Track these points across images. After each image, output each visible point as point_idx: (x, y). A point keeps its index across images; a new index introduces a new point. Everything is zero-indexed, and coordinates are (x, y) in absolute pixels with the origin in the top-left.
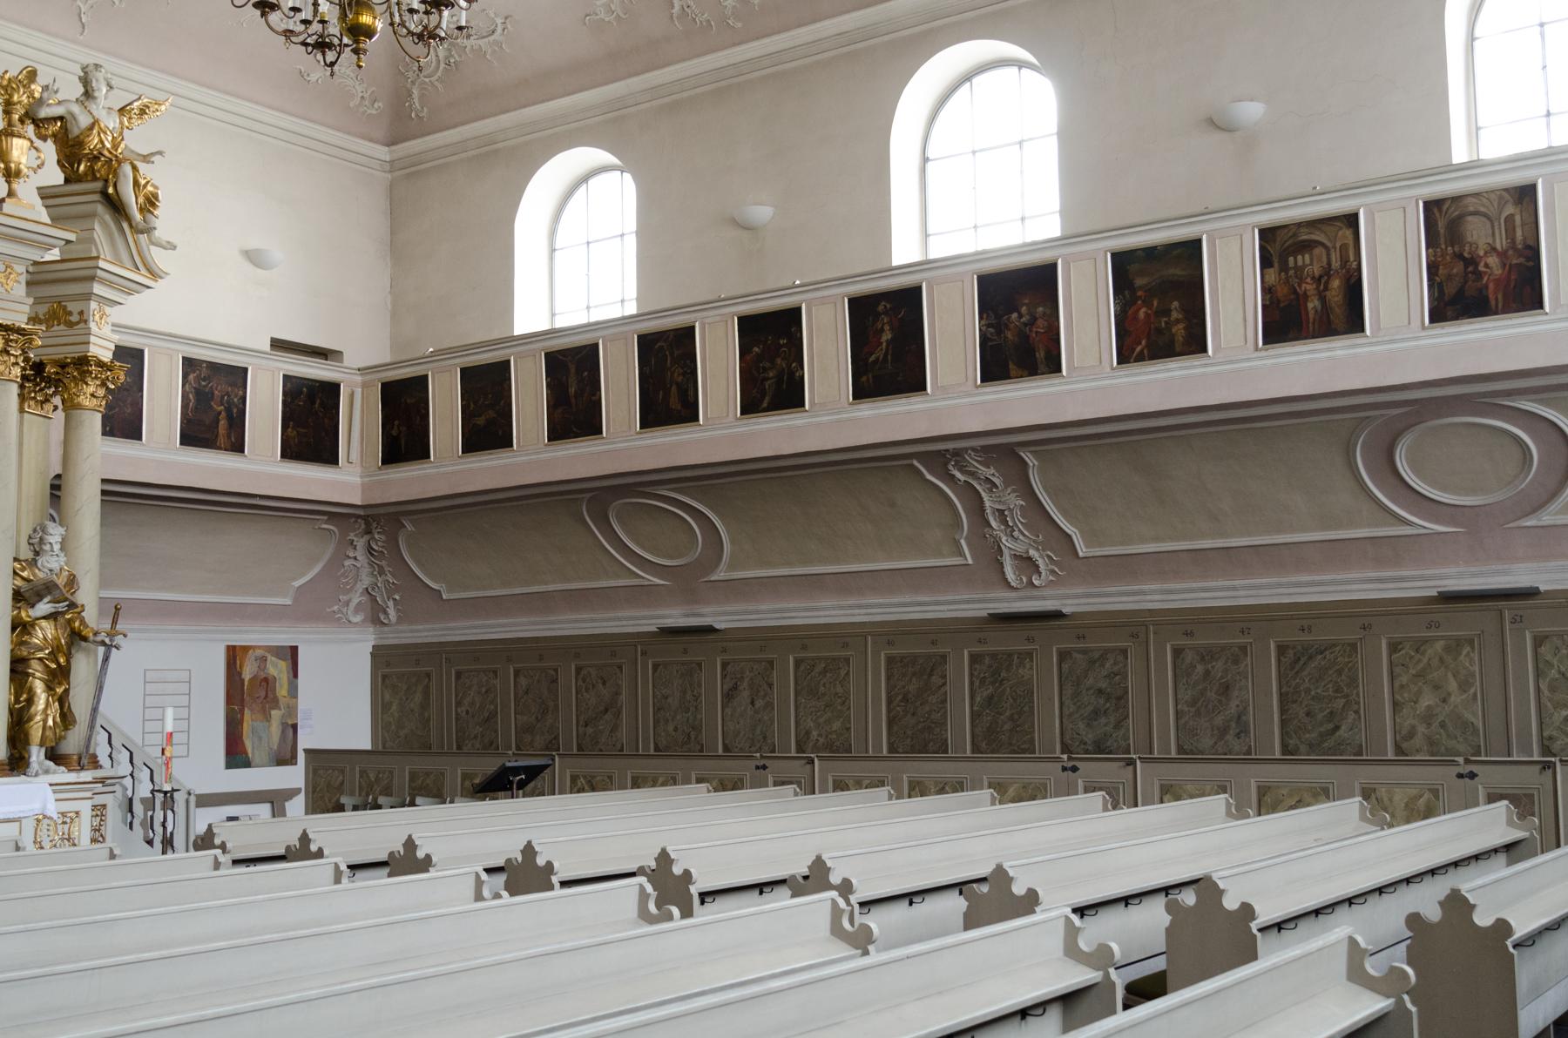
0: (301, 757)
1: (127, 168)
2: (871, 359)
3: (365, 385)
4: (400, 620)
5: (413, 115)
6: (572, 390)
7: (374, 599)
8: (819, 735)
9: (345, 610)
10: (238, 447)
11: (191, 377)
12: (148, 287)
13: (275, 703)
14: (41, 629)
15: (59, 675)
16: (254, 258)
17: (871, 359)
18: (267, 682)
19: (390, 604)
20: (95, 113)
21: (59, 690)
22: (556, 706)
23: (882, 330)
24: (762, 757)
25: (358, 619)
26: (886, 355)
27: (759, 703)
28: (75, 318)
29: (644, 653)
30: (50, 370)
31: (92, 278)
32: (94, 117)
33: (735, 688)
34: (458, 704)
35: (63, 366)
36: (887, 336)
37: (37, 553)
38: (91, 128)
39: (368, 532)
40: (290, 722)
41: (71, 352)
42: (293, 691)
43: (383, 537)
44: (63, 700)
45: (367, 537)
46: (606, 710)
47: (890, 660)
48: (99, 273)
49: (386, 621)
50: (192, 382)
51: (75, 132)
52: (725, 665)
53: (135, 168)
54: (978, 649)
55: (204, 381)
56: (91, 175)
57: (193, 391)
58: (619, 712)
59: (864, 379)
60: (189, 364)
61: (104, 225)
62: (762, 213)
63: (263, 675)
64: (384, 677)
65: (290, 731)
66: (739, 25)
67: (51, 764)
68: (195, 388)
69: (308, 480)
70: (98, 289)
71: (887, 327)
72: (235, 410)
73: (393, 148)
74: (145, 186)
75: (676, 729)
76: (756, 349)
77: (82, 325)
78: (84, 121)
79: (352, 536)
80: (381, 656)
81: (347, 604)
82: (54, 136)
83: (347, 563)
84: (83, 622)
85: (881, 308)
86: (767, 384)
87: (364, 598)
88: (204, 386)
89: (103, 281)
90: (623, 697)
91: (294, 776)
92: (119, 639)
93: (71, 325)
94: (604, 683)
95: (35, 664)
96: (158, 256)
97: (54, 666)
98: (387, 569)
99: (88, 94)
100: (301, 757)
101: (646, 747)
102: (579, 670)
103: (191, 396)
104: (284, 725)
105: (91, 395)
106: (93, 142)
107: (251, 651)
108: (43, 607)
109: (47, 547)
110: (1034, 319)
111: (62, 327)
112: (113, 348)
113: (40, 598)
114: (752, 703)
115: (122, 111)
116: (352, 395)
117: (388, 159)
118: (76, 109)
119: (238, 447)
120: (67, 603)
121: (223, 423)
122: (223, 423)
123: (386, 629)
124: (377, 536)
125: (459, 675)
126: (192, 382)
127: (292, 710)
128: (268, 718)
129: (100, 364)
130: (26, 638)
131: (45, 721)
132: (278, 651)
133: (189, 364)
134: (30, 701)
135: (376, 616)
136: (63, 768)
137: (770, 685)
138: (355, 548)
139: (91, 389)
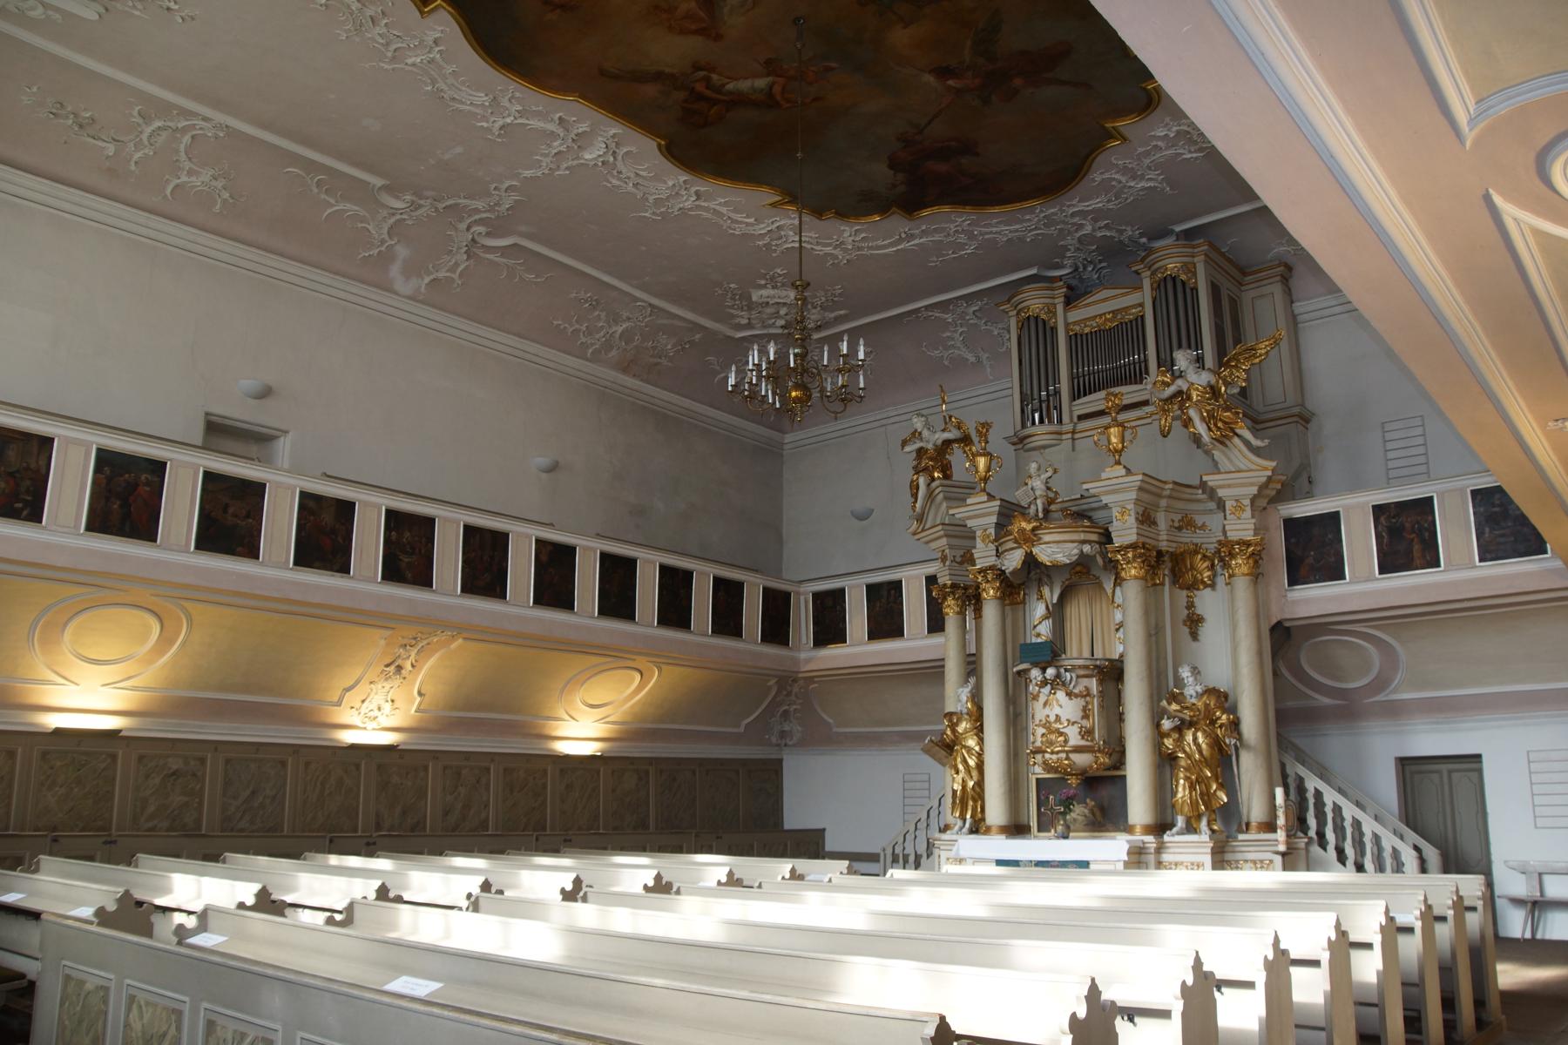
11: (1382, 519)
32: (1188, 382)
50: (1384, 522)
55: (1393, 518)
57: (1385, 529)
68: (1386, 527)
72: (1427, 534)
88: (1395, 523)
103: (1384, 534)
121: (1416, 547)
122: (1416, 547)
126: (1384, 522)
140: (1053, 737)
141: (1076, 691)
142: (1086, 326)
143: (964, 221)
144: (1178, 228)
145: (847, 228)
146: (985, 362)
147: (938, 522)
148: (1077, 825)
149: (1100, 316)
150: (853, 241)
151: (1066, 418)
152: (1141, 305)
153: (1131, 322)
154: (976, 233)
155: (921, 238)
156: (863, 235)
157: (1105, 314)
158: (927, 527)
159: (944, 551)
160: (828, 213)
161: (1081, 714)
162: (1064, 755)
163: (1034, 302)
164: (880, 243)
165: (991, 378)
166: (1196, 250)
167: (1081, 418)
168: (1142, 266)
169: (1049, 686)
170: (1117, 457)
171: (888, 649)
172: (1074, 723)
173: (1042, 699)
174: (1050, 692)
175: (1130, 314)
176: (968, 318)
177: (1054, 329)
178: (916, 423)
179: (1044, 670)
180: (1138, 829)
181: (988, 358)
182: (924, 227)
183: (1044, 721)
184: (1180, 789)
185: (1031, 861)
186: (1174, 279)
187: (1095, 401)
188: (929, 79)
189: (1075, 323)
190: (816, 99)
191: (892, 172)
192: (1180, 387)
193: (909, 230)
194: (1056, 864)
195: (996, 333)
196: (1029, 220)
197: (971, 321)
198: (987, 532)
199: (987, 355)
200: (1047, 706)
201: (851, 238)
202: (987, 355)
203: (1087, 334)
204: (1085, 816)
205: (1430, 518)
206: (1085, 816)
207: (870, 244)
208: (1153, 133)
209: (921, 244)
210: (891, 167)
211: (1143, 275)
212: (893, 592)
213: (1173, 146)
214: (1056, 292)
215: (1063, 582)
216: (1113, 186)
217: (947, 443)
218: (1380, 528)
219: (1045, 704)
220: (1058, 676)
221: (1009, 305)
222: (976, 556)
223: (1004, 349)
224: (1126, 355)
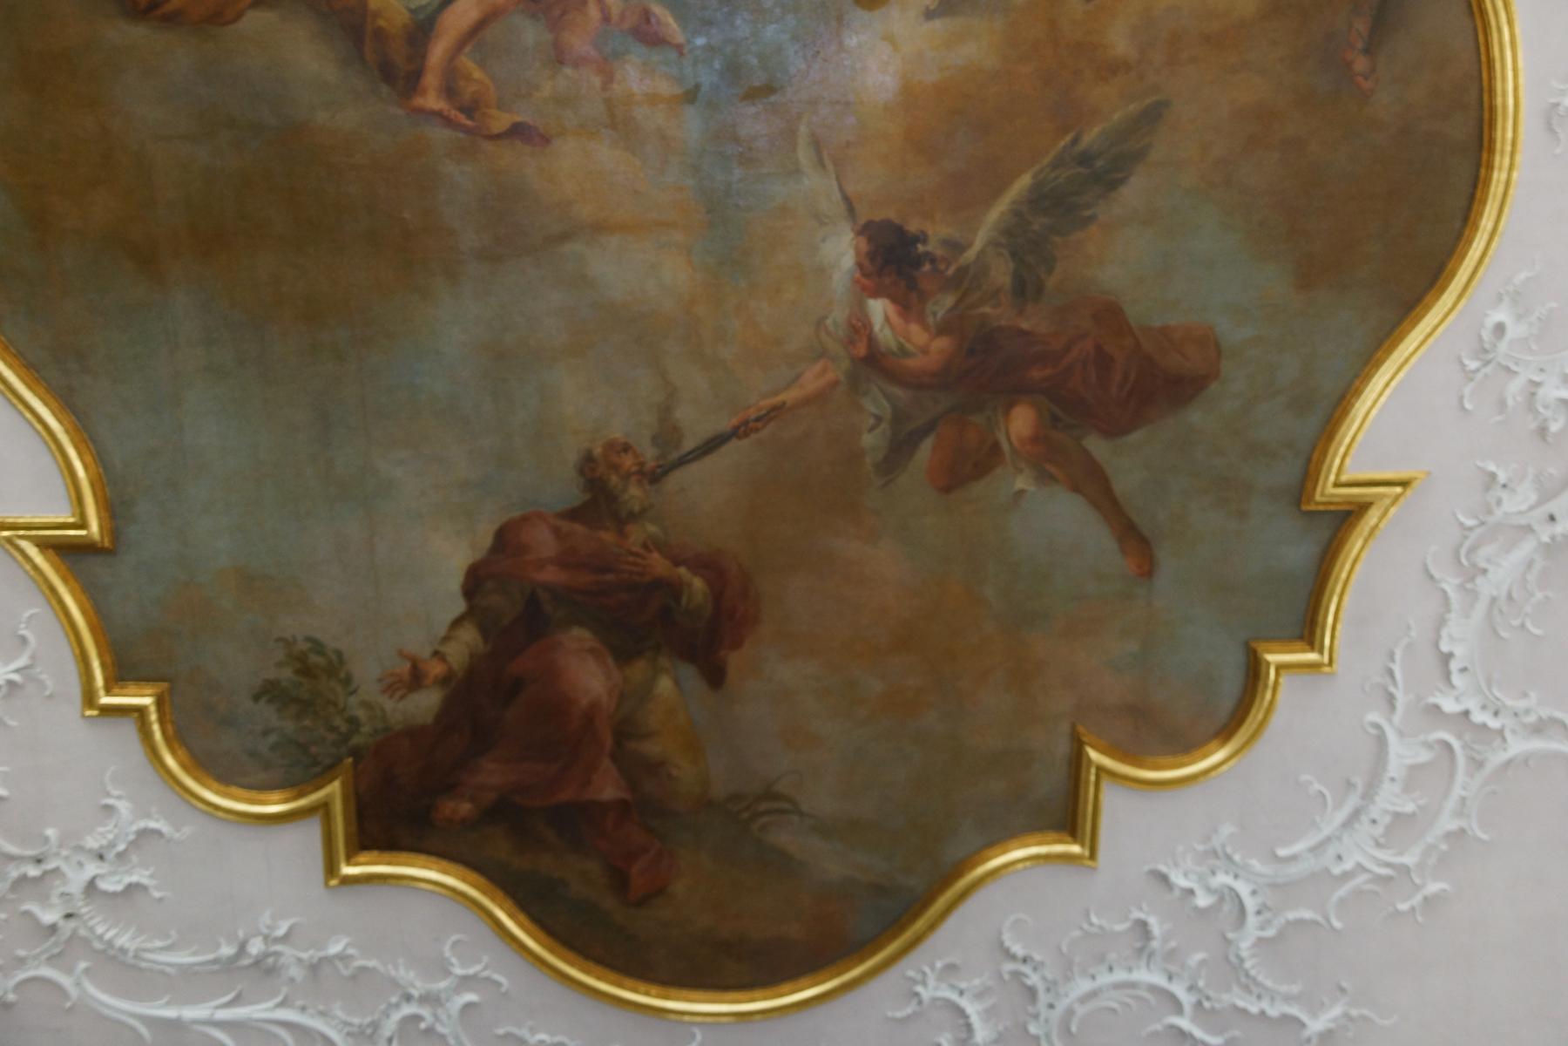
143: (466, 982)
145: (124, 807)
155: (283, 1004)
182: (335, 949)
190: (518, 132)
191: (459, 606)
193: (285, 939)
201: (92, 869)
207: (124, 941)
208: (1163, 869)
210: (475, 581)
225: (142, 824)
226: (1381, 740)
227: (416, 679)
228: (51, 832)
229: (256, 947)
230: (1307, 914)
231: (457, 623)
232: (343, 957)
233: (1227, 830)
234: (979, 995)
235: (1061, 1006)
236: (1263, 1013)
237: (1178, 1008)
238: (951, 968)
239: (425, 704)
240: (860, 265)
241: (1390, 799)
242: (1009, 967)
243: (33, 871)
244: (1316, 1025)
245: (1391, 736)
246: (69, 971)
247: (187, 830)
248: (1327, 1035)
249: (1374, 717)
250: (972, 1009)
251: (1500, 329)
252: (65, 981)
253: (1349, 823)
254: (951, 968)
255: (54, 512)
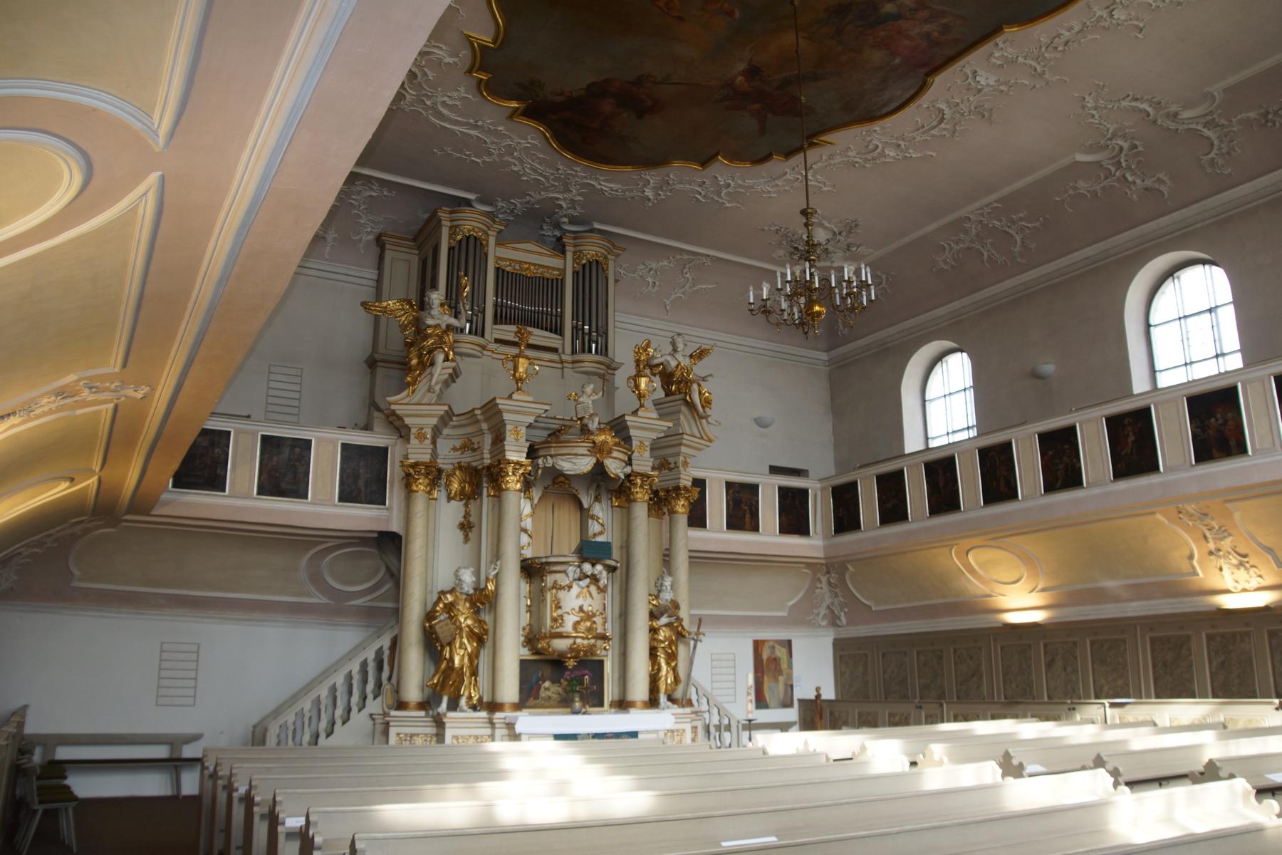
0: (796, 703)
1: (695, 387)
2: (1123, 454)
3: (822, 489)
4: (848, 624)
5: (840, 333)
6: (941, 485)
7: (832, 612)
8: (1110, 689)
9: (817, 618)
10: (755, 528)
11: (731, 492)
12: (708, 446)
13: (780, 672)
14: (663, 631)
15: (672, 657)
16: (760, 423)
17: (1123, 454)
18: (775, 661)
19: (842, 614)
20: (678, 358)
21: (673, 664)
22: (943, 675)
23: (1128, 435)
24: (1072, 703)
25: (824, 623)
26: (1132, 450)
27: (1069, 669)
28: (672, 466)
29: (995, 640)
30: (662, 494)
31: (680, 444)
33: (1053, 660)
34: (884, 672)
35: (667, 491)
36: (1131, 438)
37: (659, 591)
38: (677, 367)
39: (828, 572)
40: (789, 683)
41: (671, 484)
42: (790, 666)
43: (837, 576)
44: (674, 670)
45: (828, 576)
46: (973, 675)
47: (1153, 640)
48: (684, 441)
49: (840, 624)
51: (670, 370)
52: (1045, 646)
53: (699, 385)
54: (1211, 631)
55: (737, 492)
56: (679, 391)
58: (982, 677)
59: (1119, 465)
60: (729, 485)
61: (685, 416)
62: (1049, 368)
63: (773, 656)
64: (841, 657)
65: (789, 689)
66: (1024, 261)
67: (669, 704)
69: (794, 543)
70: (683, 449)
71: (1131, 433)
73: (830, 353)
74: (704, 394)
75: (1017, 686)
76: (1050, 452)
77: (676, 469)
78: (673, 364)
79: (819, 575)
80: (839, 645)
81: (818, 614)
82: (660, 373)
83: (817, 591)
84: (683, 628)
85: (1126, 422)
86: (1059, 473)
87: (827, 612)
89: (685, 445)
90: (983, 668)
91: (792, 714)
92: (701, 637)
93: (670, 469)
94: (971, 658)
95: (660, 649)
96: (711, 431)
97: (670, 651)
98: (840, 594)
99: (675, 350)
100: (796, 703)
101: (999, 697)
102: (955, 651)
104: (786, 685)
105: (681, 506)
106: (678, 373)
107: (766, 643)
108: (664, 620)
109: (664, 588)
110: (1226, 422)
111: (667, 471)
112: (691, 479)
113: (662, 614)
114: (1065, 669)
115: (691, 356)
116: (815, 496)
117: (827, 359)
118: (669, 358)
119: (755, 528)
120: (675, 618)
121: (748, 516)
122: (748, 516)
123: (840, 629)
124: (833, 575)
125: (884, 655)
127: (790, 676)
128: (777, 681)
129: (685, 488)
130: (656, 636)
131: (666, 680)
132: (781, 643)
133: (729, 485)
134: (659, 670)
135: (834, 622)
136: (676, 706)
137: (1075, 658)
138: (821, 582)
139: (682, 503)
140: (588, 624)
141: (602, 587)
142: (510, 265)
143: (529, 143)
144: (597, 226)
145: (462, 90)
146: (329, 240)
147: (423, 402)
148: (552, 702)
149: (526, 263)
150: (445, 102)
151: (487, 335)
152: (563, 271)
153: (548, 279)
154: (515, 154)
155: (480, 133)
156: (458, 103)
157: (529, 263)
158: (413, 401)
159: (422, 429)
160: (485, 74)
161: (602, 608)
162: (593, 641)
163: (471, 223)
164: (454, 117)
165: (327, 257)
166: (614, 251)
167: (497, 341)
168: (572, 242)
169: (588, 580)
170: (520, 384)
171: (281, 509)
172: (602, 614)
173: (575, 589)
174: (588, 587)
175: (548, 273)
176: (354, 197)
177: (486, 255)
178: (436, 299)
179: (593, 565)
180: (639, 704)
181: (335, 239)
183: (577, 609)
184: (664, 672)
185: (589, 734)
186: (597, 261)
187: (508, 332)
188: (742, 66)
189: (500, 259)
191: (585, 87)
192: (668, 362)
194: (611, 735)
195: (362, 222)
196: (559, 169)
197: (351, 201)
198: (519, 429)
199: (336, 236)
200: (581, 598)
201: (446, 99)
202: (336, 236)
203: (508, 272)
204: (559, 694)
205: (756, 498)
206: (559, 694)
209: (470, 135)
211: (567, 248)
212: (297, 450)
213: (705, 188)
214: (495, 226)
215: (546, 488)
216: (639, 184)
217: (449, 328)
218: (728, 498)
219: (578, 596)
220: (601, 573)
221: (448, 216)
222: (507, 447)
223: (355, 238)
224: (537, 305)
225: (465, 95)
226: (786, 173)
227: (561, 94)
228: (439, 89)
229: (480, 123)
230: (742, 190)
231: (582, 89)
232: (501, 131)
233: (738, 174)
234: (655, 180)
235: (673, 187)
236: (718, 201)
237: (700, 194)
238: (652, 175)
239: (559, 99)
240: (743, 71)
241: (780, 182)
242: (667, 178)
243: (429, 94)
244: (728, 205)
245: (788, 173)
246: (426, 111)
247: (477, 99)
248: (727, 207)
249: (787, 170)
250: (652, 181)
251: (876, 131)
252: (424, 113)
253: (766, 182)
254: (652, 175)
255: (487, 39)
